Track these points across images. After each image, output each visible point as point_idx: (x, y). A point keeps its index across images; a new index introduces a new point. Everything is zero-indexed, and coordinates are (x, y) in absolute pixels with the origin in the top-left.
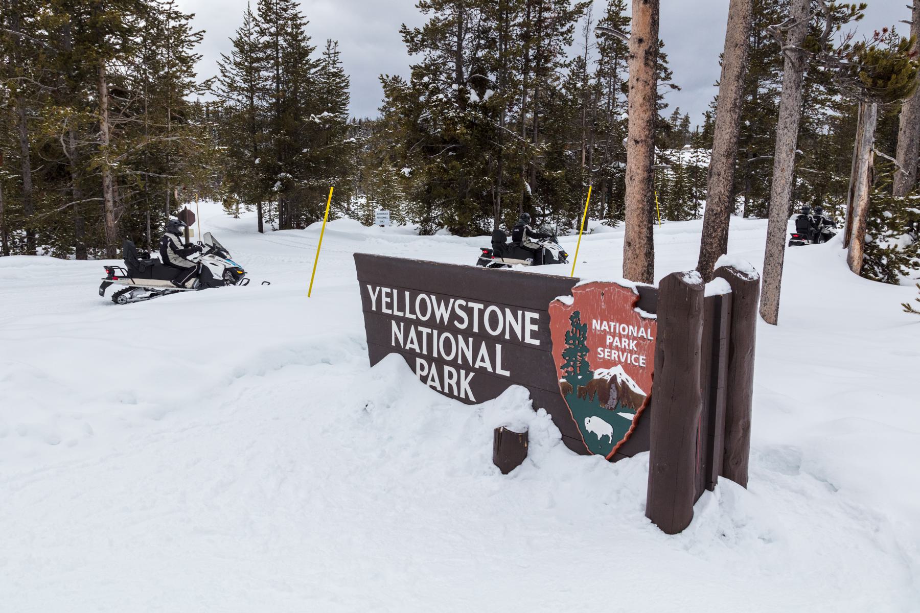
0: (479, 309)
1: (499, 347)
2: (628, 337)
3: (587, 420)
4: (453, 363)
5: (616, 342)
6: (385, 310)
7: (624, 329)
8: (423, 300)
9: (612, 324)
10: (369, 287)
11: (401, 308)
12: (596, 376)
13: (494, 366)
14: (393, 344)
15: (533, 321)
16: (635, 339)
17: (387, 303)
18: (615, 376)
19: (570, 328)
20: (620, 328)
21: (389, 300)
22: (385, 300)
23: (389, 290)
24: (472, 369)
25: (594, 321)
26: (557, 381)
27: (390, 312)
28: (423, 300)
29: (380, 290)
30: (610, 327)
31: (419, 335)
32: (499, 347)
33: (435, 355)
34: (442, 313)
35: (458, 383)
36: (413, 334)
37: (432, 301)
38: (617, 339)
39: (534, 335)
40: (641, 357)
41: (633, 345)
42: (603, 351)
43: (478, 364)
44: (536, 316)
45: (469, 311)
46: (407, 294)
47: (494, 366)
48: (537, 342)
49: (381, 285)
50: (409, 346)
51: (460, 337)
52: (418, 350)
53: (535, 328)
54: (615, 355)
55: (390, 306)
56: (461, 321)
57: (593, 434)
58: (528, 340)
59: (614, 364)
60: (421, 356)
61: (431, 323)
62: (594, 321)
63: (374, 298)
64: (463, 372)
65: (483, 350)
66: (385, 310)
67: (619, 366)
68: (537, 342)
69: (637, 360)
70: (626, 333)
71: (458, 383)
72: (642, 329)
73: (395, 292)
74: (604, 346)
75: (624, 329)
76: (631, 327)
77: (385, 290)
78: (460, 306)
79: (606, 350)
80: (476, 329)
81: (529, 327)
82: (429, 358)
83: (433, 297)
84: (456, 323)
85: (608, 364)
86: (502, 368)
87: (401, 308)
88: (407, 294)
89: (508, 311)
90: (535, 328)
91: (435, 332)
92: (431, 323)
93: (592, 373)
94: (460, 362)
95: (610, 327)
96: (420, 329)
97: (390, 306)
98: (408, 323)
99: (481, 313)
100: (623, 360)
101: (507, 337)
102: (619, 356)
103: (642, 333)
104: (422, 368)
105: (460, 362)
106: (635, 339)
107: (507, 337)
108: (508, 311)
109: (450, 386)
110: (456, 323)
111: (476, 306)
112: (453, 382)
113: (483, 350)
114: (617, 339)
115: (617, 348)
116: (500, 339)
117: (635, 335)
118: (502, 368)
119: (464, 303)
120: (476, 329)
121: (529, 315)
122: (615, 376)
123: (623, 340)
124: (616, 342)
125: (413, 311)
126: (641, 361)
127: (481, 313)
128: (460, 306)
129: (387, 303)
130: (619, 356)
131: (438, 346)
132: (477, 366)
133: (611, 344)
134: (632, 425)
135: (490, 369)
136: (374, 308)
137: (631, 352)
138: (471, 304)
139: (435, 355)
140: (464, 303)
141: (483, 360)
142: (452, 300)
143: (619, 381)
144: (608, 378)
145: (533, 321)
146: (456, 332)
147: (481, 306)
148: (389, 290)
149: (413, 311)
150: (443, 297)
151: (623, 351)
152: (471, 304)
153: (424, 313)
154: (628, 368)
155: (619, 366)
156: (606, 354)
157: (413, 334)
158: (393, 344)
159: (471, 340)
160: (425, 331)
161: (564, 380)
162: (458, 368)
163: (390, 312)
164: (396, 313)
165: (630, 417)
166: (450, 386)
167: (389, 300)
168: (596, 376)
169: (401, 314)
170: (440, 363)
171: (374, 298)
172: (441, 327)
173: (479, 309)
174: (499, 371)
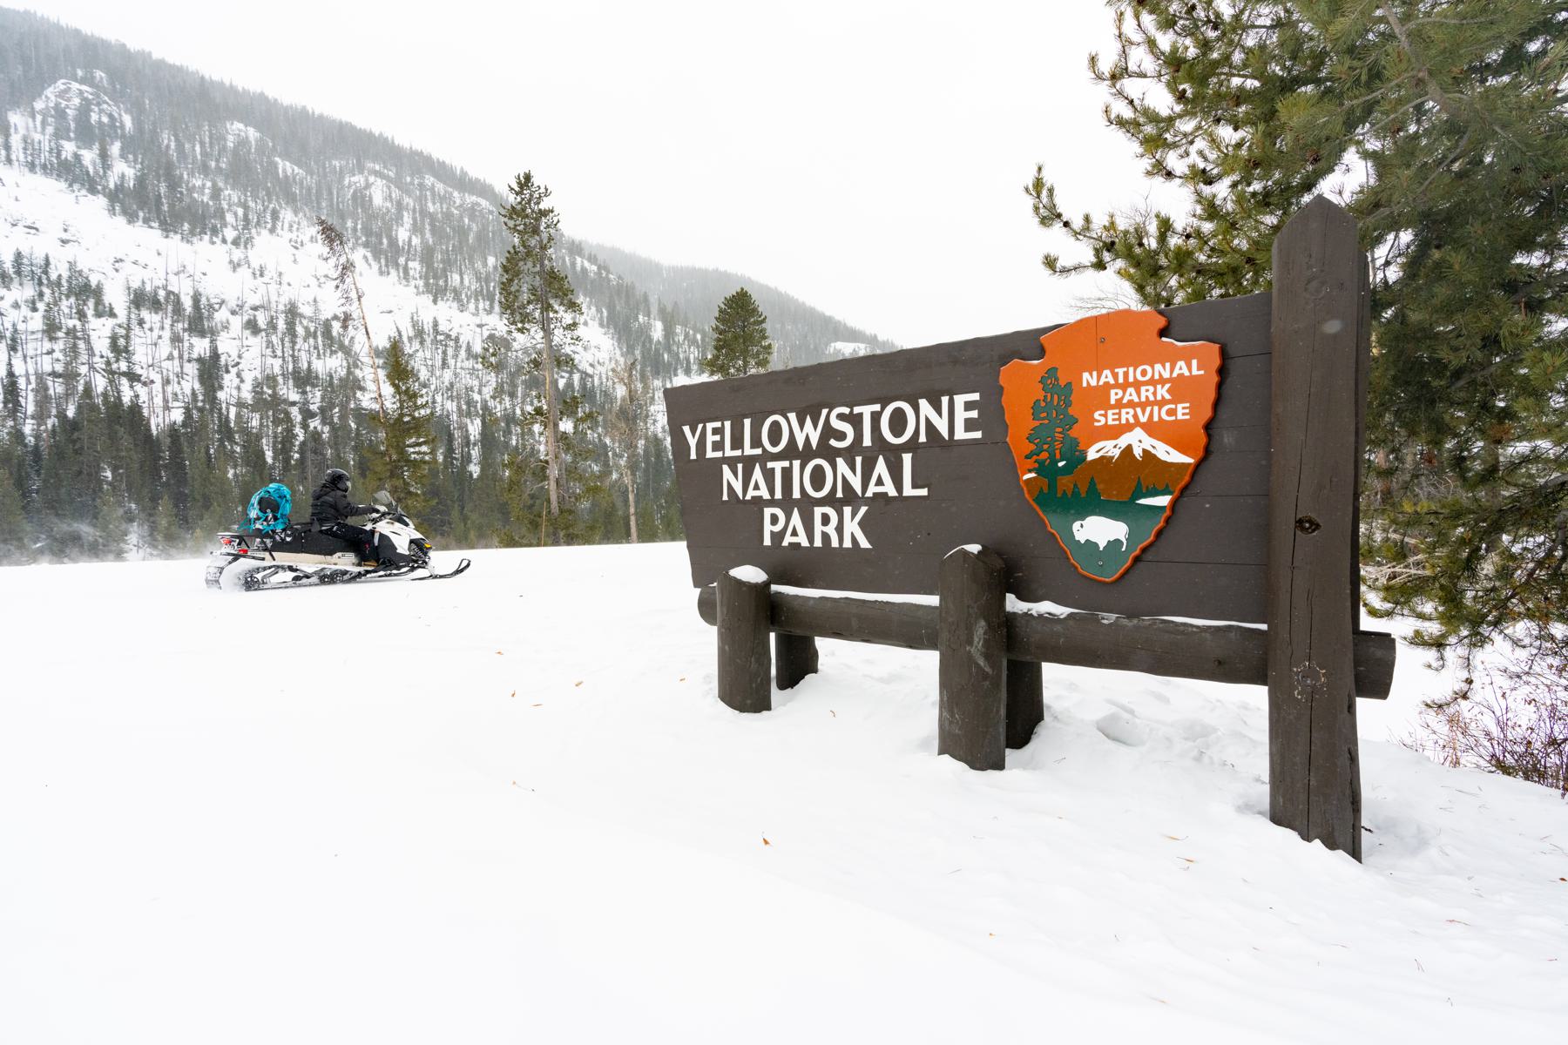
1: (907, 458)
2: (1152, 382)
3: (1076, 525)
4: (830, 500)
5: (1131, 395)
6: (710, 454)
7: (1144, 373)
8: (776, 425)
9: (1121, 371)
10: (686, 429)
11: (737, 443)
12: (1092, 455)
13: (898, 484)
14: (725, 498)
15: (969, 406)
16: (1162, 381)
18: (1129, 448)
19: (1041, 395)
20: (1134, 374)
21: (717, 438)
22: (711, 438)
23: (718, 424)
24: (867, 501)
25: (1086, 375)
26: (1018, 478)
27: (719, 454)
28: (776, 425)
30: (1115, 376)
31: (769, 475)
32: (907, 458)
33: (796, 494)
34: (810, 433)
35: (840, 529)
36: (757, 474)
37: (789, 423)
38: (1131, 390)
39: (970, 425)
40: (1180, 406)
41: (1163, 392)
42: (1105, 416)
43: (872, 489)
45: (856, 421)
46: (747, 422)
47: (898, 484)
48: (978, 435)
49: (704, 422)
50: (751, 493)
51: (840, 461)
52: (766, 496)
53: (974, 414)
54: (1127, 415)
55: (718, 446)
56: (841, 436)
57: (1090, 544)
58: (960, 434)
59: (1128, 428)
60: (772, 503)
61: (791, 452)
62: (1086, 375)
63: (693, 442)
64: (847, 510)
65: (881, 467)
66: (710, 454)
67: (1138, 430)
68: (978, 435)
69: (1171, 412)
70: (1148, 377)
71: (840, 529)
72: (1181, 363)
73: (728, 424)
74: (1106, 406)
75: (1144, 373)
76: (1158, 367)
77: (710, 426)
78: (841, 417)
79: (1110, 412)
80: (867, 442)
81: (961, 415)
82: (787, 504)
83: (792, 416)
84: (833, 442)
85: (1115, 432)
86: (914, 486)
87: (737, 443)
88: (747, 422)
89: (923, 403)
90: (974, 414)
91: (797, 464)
92: (791, 452)
93: (1084, 454)
94: (839, 494)
95: (1115, 376)
96: (770, 465)
98: (749, 463)
99: (876, 417)
100: (1143, 419)
101: (923, 438)
102: (1135, 416)
103: (1181, 368)
104: (774, 520)
105: (839, 494)
106: (1162, 381)
107: (923, 438)
108: (924, 404)
109: (826, 537)
110: (833, 442)
111: (866, 411)
112: (831, 529)
113: (881, 467)
114: (1131, 390)
115: (1131, 404)
116: (912, 446)
117: (1166, 375)
118: (914, 486)
119: (846, 410)
120: (867, 442)
121: (960, 400)
122: (1129, 448)
123: (1143, 389)
124: (1131, 395)
125: (756, 442)
126: (1180, 411)
127: (876, 417)
130: (1135, 416)
131: (801, 479)
132: (869, 494)
133: (1119, 401)
134: (1168, 513)
135: (892, 492)
136: (693, 456)
137: (1163, 402)
138: (857, 410)
139: (796, 494)
140: (846, 410)
141: (880, 482)
142: (825, 412)
143: (1138, 452)
144: (1116, 453)
145: (969, 406)
146: (831, 455)
147: (877, 407)
148: (718, 424)
149: (756, 442)
150: (808, 411)
151: (1143, 406)
152: (857, 410)
153: (775, 442)
154: (1151, 428)
155: (1138, 430)
156: (1110, 417)
157: (757, 474)
158: (725, 498)
159: (859, 460)
160: (778, 466)
161: (1033, 475)
162: (838, 505)
163: (719, 454)
164: (729, 453)
165: (1163, 501)
166: (826, 537)
167: (717, 438)
168: (1092, 455)
169: (738, 453)
170: (806, 506)
171: (693, 442)
172: (806, 454)
174: (908, 491)
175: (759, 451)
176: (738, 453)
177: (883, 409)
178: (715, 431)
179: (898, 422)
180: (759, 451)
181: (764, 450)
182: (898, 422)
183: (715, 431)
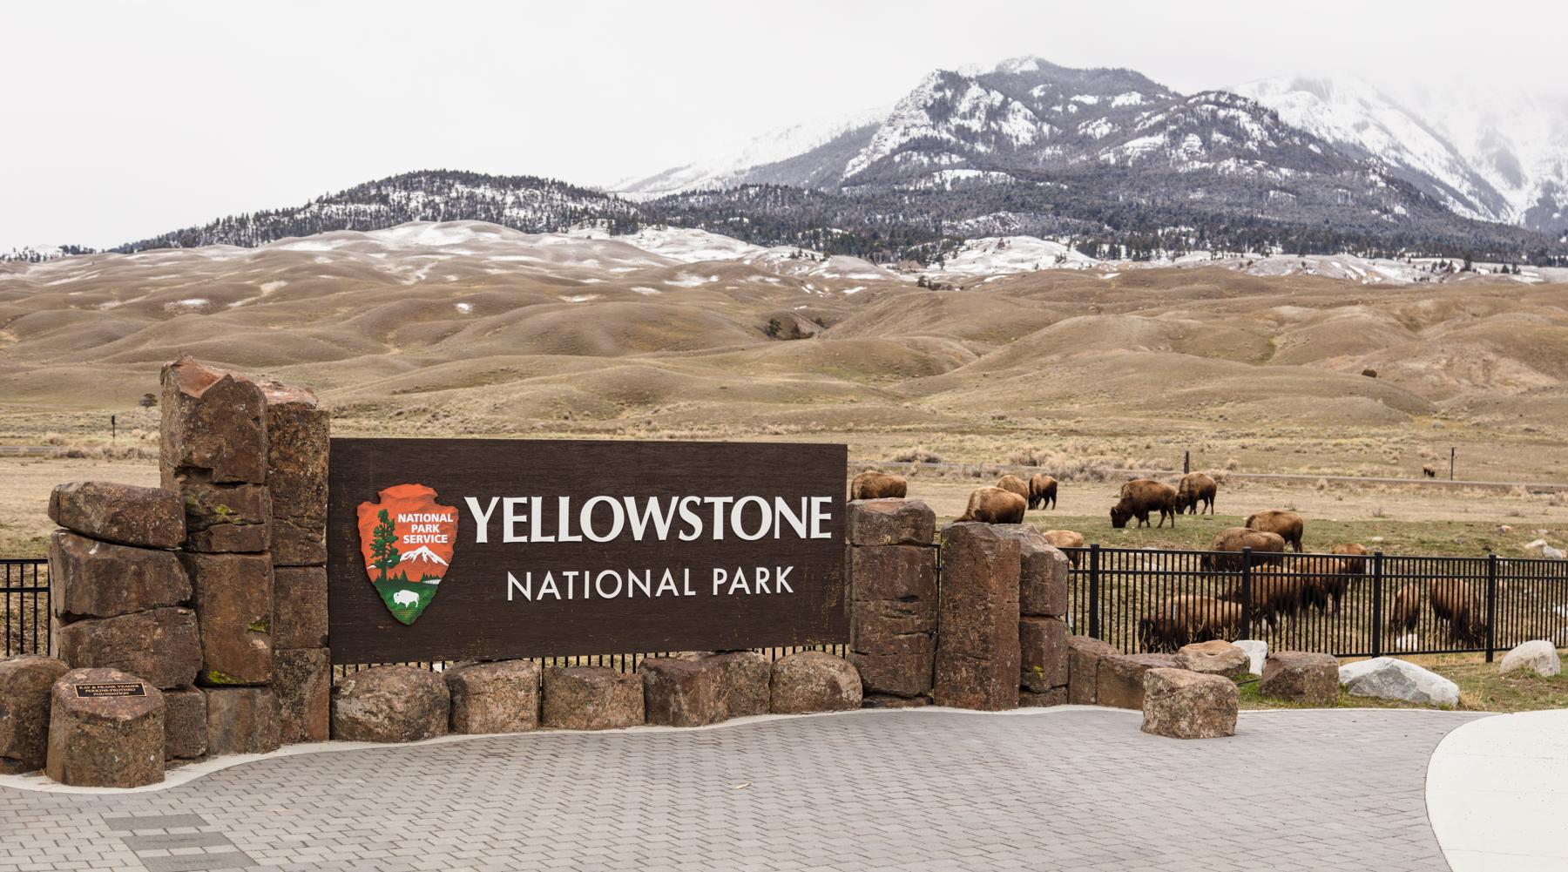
0: (725, 504)
6: (509, 536)
11: (550, 525)
17: (515, 523)
21: (523, 518)
22: (509, 519)
23: (524, 500)
29: (500, 506)
44: (829, 499)
45: (705, 512)
49: (502, 495)
63: (482, 521)
73: (537, 502)
77: (509, 503)
83: (630, 502)
89: (779, 501)
97: (521, 529)
99: (728, 508)
101: (777, 536)
108: (779, 501)
111: (719, 502)
119: (697, 500)
129: (515, 523)
136: (482, 537)
138: (708, 500)
147: (730, 499)
148: (524, 500)
152: (708, 500)
167: (523, 518)
171: (482, 521)
173: (725, 504)
177: (736, 500)
179: (752, 517)
182: (752, 517)
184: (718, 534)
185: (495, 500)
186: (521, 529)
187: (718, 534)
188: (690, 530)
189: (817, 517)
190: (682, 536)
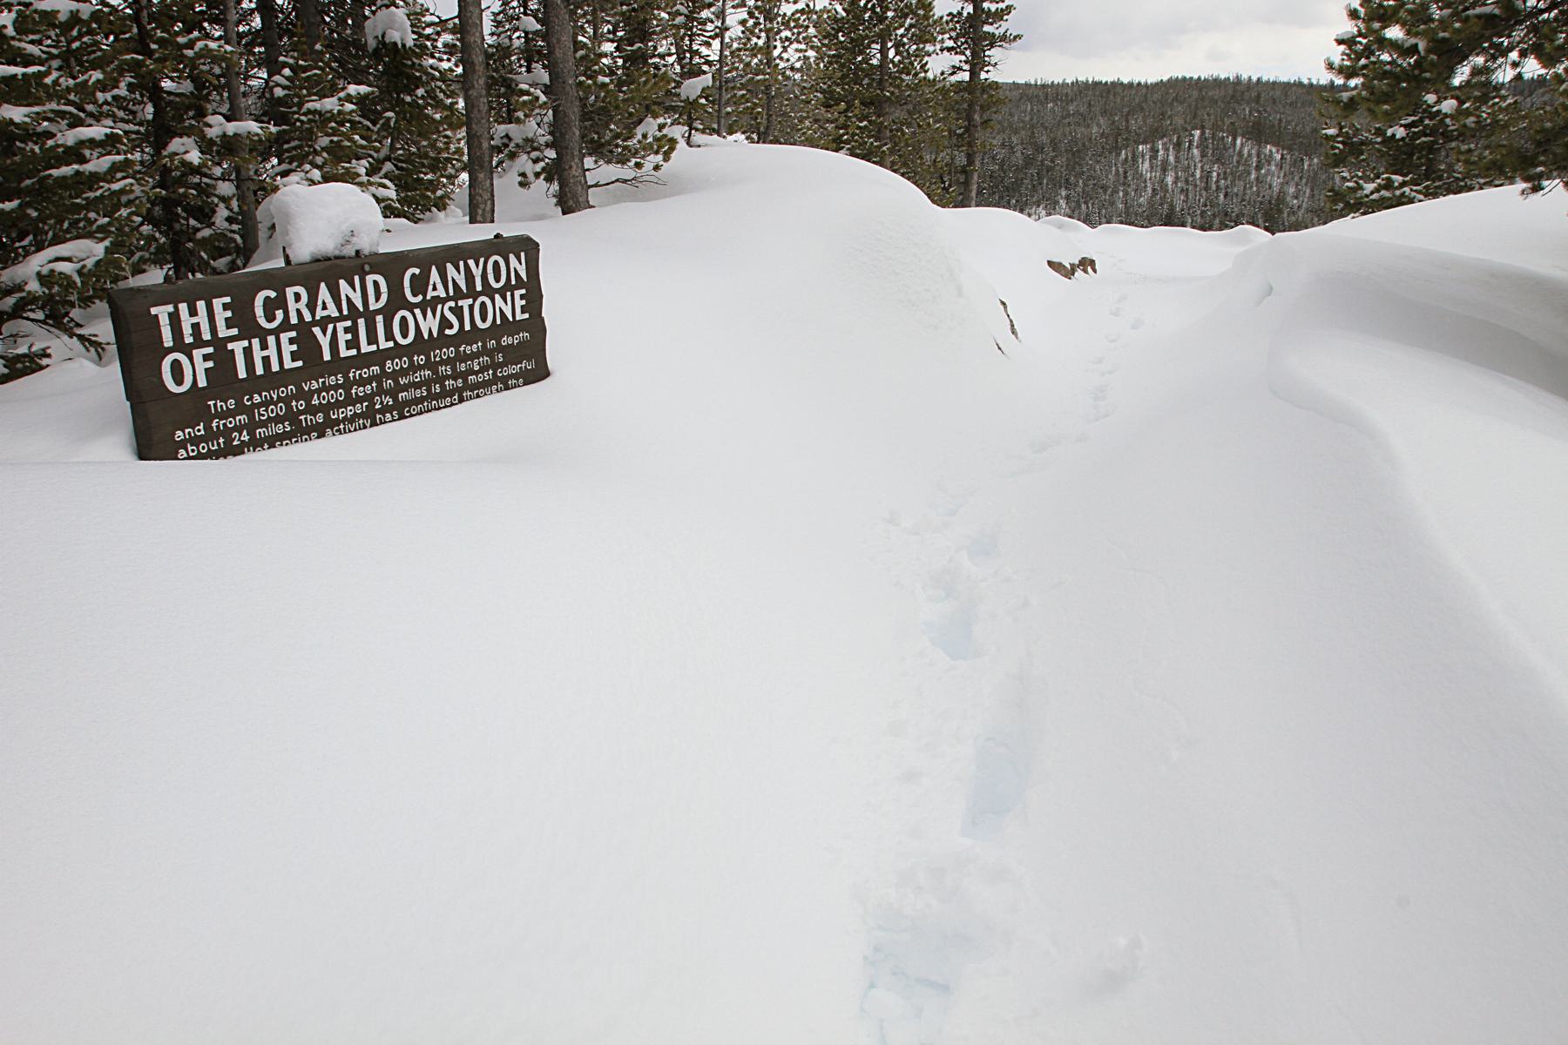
6: (344, 353)
8: (404, 319)
11: (372, 339)
21: (349, 336)
22: (343, 337)
27: (354, 352)
28: (404, 319)
63: (325, 342)
66: (344, 353)
87: (372, 339)
97: (353, 343)
99: (471, 307)
125: (389, 336)
127: (471, 307)
128: (450, 309)
136: (327, 357)
138: (460, 303)
147: (470, 301)
149: (389, 336)
152: (460, 303)
167: (349, 336)
169: (373, 348)
175: (391, 344)
176: (373, 348)
178: (347, 330)
180: (391, 344)
181: (396, 342)
183: (347, 330)
184: (467, 327)
185: (331, 326)
186: (353, 343)
187: (467, 327)
188: (451, 326)
189: (519, 303)
190: (448, 332)
